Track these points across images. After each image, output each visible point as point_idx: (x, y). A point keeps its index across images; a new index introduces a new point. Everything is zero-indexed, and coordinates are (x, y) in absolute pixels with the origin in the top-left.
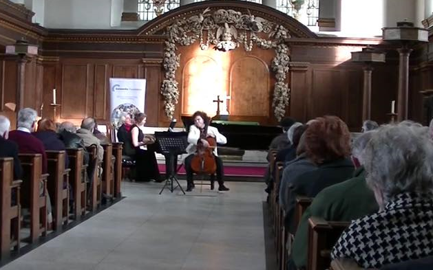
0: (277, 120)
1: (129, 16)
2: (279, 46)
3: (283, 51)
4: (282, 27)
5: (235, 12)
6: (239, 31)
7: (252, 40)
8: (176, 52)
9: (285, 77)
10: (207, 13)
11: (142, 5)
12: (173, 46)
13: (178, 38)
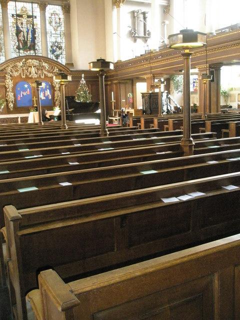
6: (38, 69)
8: (11, 79)
12: (9, 76)
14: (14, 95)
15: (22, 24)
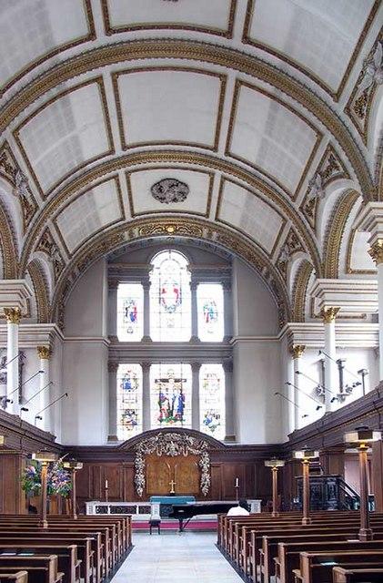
1: (112, 438)
15: (167, 389)
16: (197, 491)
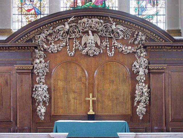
0: (139, 117)
2: (139, 51)
3: (142, 55)
4: (140, 33)
5: (98, 20)
7: (114, 46)
9: (144, 79)
10: (72, 22)
11: (17, 23)
13: (45, 46)
14: (49, 90)
16: (129, 112)
